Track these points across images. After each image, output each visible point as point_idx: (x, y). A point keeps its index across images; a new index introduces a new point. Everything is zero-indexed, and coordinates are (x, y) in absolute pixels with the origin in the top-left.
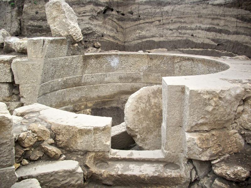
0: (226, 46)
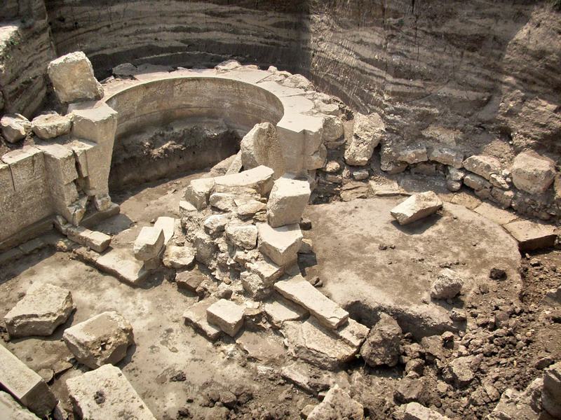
0: (198, 46)
